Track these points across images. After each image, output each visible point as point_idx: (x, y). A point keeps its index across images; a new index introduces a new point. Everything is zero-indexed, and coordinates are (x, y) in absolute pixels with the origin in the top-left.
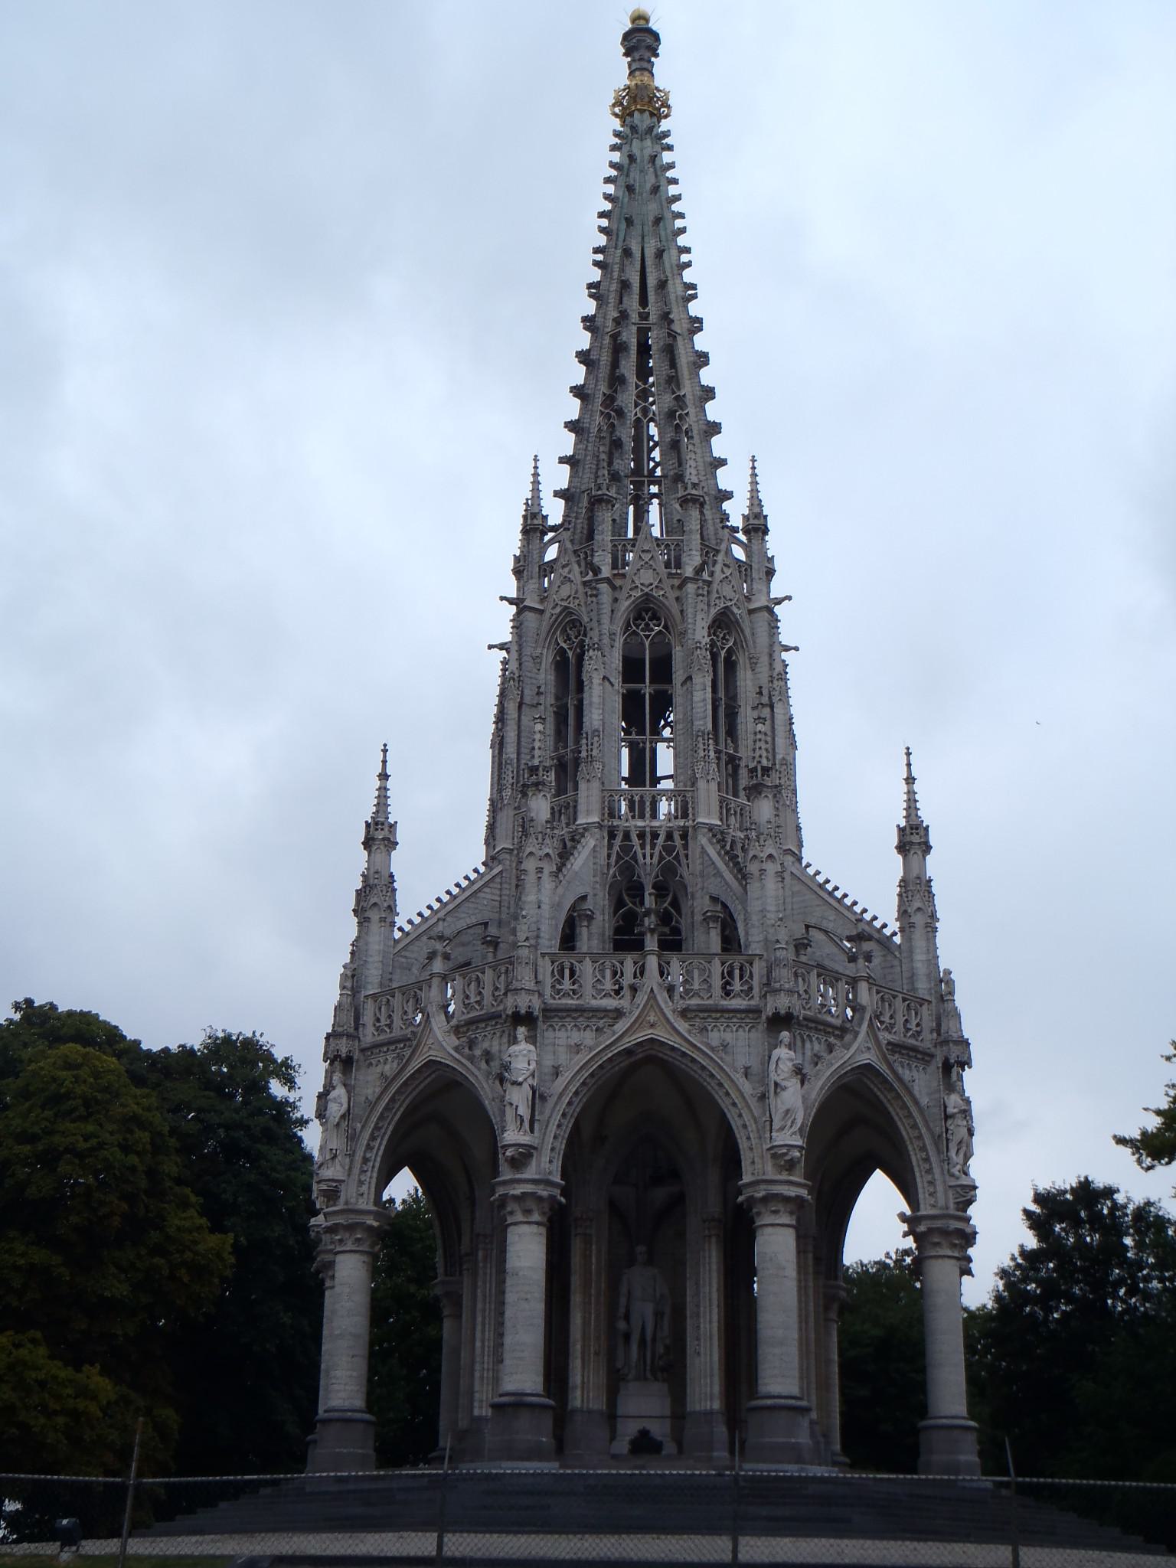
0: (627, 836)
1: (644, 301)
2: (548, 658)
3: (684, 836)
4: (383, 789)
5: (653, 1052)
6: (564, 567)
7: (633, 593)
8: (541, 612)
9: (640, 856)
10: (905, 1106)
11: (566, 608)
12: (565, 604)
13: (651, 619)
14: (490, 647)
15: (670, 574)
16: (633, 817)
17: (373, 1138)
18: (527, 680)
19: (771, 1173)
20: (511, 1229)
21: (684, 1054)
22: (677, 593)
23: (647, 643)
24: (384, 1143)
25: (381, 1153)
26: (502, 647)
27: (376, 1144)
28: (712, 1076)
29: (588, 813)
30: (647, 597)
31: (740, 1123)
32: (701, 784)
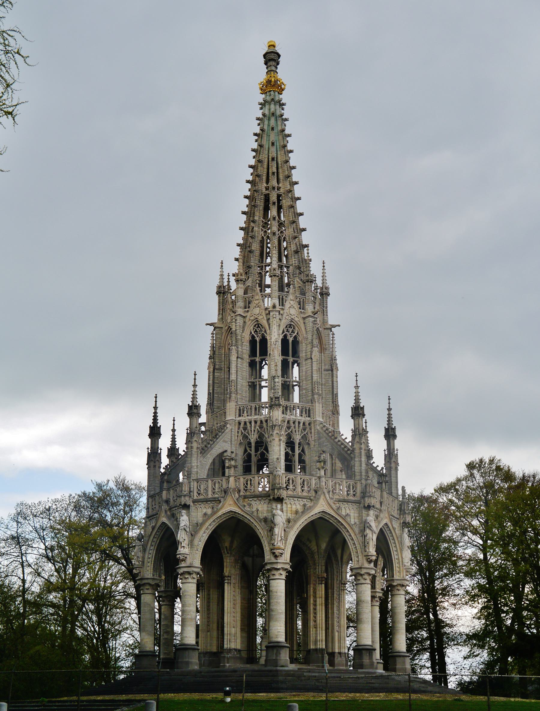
0: (288, 422)
1: (278, 182)
4: (194, 391)
8: (244, 317)
9: (294, 430)
10: (393, 539)
12: (256, 317)
14: (207, 324)
26: (211, 325)
32: (317, 404)
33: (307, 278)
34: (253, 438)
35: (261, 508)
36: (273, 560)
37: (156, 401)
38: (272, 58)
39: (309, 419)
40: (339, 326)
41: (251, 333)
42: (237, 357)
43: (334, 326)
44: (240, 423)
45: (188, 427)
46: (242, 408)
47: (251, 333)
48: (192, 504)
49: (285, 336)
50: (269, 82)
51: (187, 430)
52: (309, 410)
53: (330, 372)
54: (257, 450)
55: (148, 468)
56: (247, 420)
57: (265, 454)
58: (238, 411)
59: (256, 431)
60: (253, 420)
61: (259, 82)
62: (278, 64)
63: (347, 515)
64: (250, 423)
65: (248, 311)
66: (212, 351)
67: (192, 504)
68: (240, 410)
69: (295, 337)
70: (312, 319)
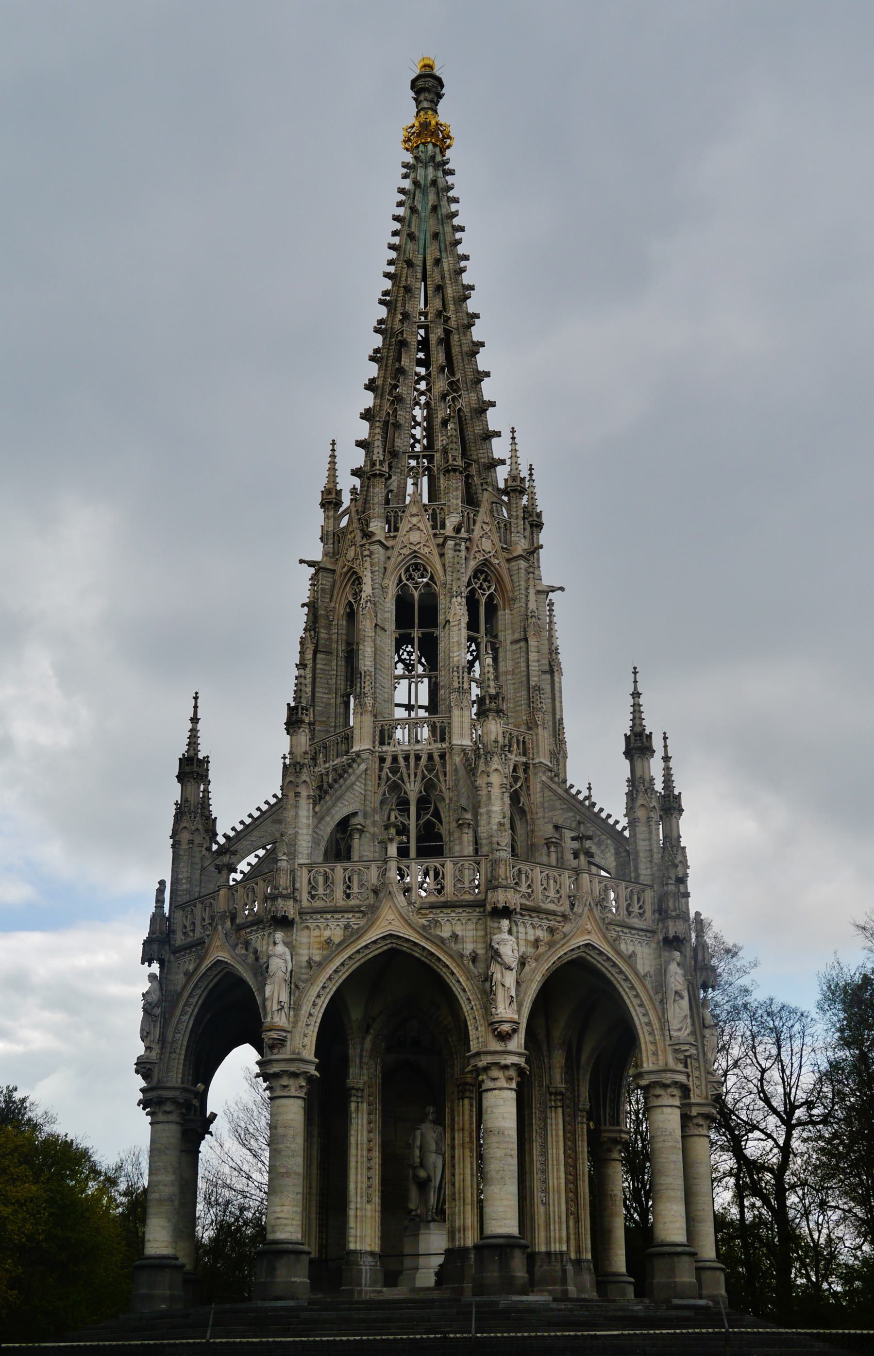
2: (392, 591)
3: (525, 771)
5: (584, 954)
6: (412, 516)
7: (477, 555)
11: (415, 552)
12: (416, 548)
13: (485, 580)
14: (302, 561)
15: (502, 548)
16: (435, 741)
17: (319, 996)
18: (378, 605)
19: (672, 1064)
20: (484, 1094)
21: (609, 959)
22: (507, 566)
23: (483, 600)
24: (327, 1001)
25: (322, 1010)
26: (311, 564)
27: (319, 1001)
28: (627, 979)
29: (462, 736)
30: (486, 563)
31: (644, 1020)
33: (514, 484)
34: (413, 789)
35: (464, 930)
36: (495, 1045)
37: (196, 707)
38: (427, 87)
39: (524, 759)
40: (562, 589)
41: (400, 580)
42: (376, 625)
43: (553, 590)
44: (382, 760)
45: (287, 751)
46: (386, 728)
47: (400, 580)
48: (297, 919)
49: (472, 592)
50: (425, 125)
51: (284, 758)
52: (524, 742)
53: (548, 676)
54: (418, 818)
55: (173, 846)
56: (400, 753)
57: (434, 824)
58: (378, 733)
59: (419, 778)
60: (412, 752)
61: (405, 127)
62: (440, 96)
63: (633, 954)
64: (407, 758)
65: (395, 537)
66: (311, 615)
67: (297, 919)
68: (382, 732)
69: (491, 597)
70: (523, 564)
